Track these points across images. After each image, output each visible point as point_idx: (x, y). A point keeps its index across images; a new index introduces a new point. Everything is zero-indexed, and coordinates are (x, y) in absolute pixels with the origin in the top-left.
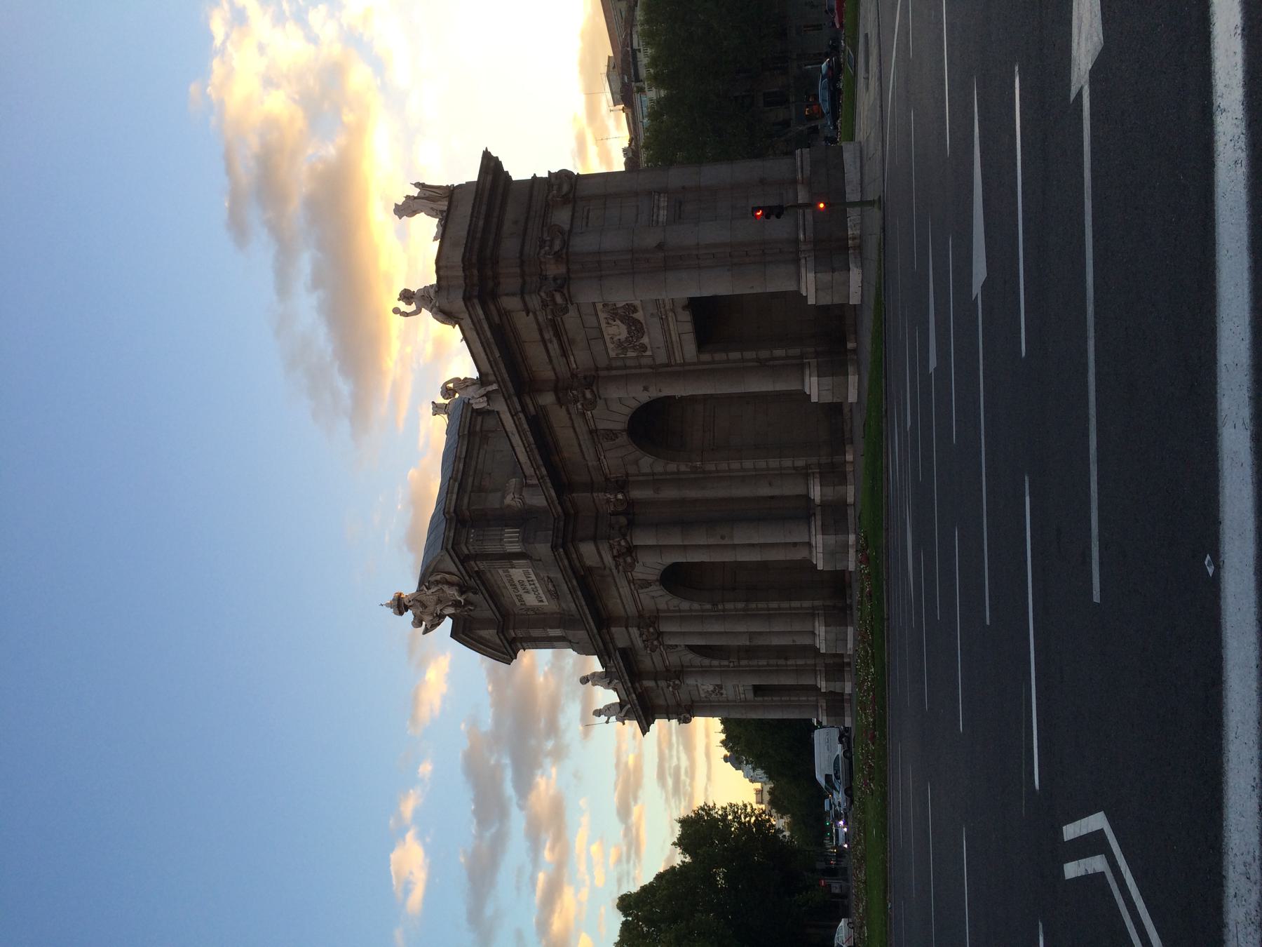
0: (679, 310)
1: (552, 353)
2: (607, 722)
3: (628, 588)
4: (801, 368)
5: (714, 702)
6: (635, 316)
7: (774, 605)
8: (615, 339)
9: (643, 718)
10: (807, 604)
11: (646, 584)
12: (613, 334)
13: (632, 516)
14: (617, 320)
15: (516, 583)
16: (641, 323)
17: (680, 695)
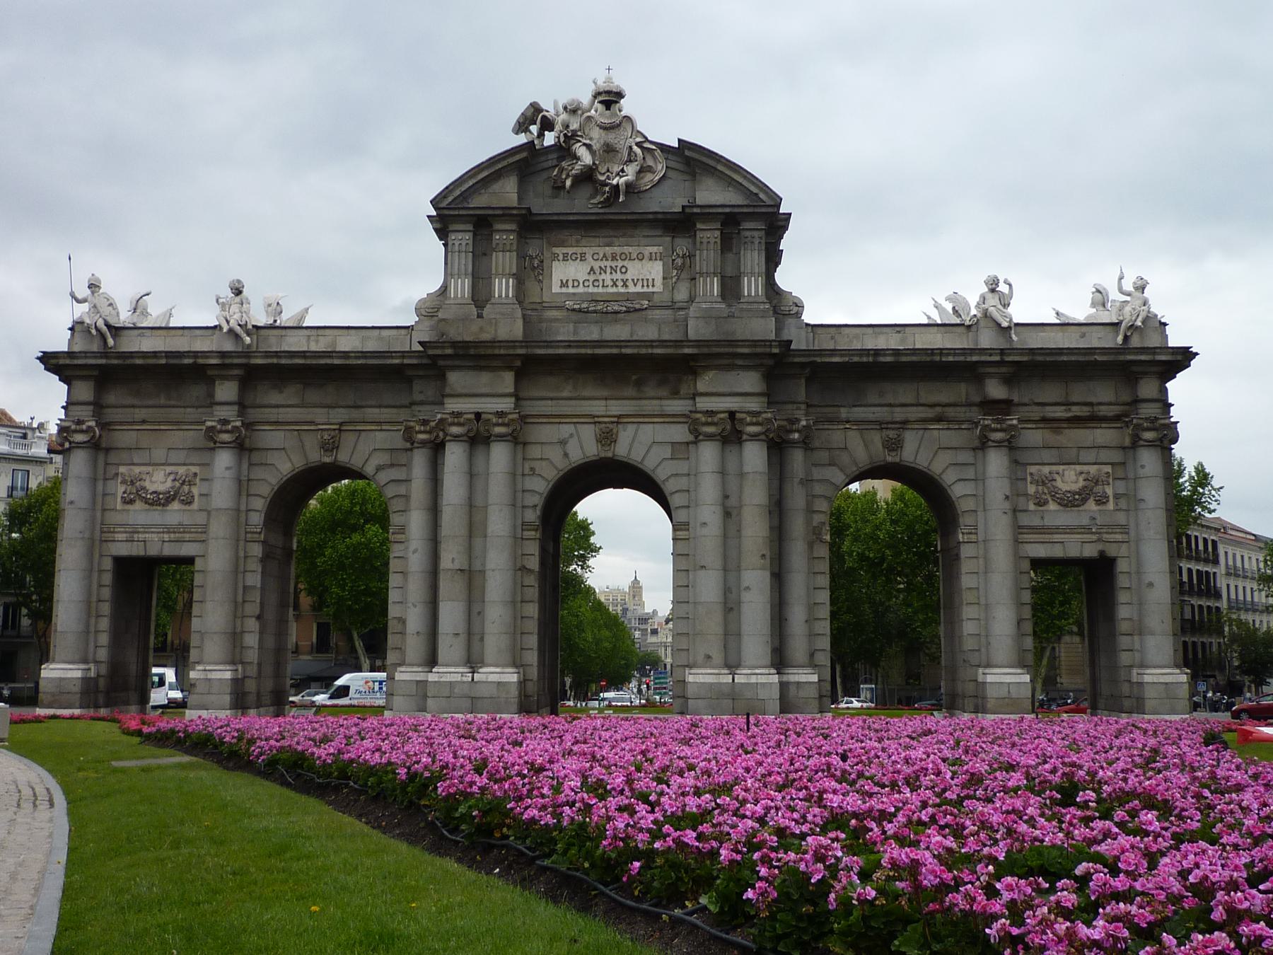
0: (1100, 547)
1: (1048, 408)
2: (73, 296)
3: (603, 413)
4: (1021, 664)
5: (104, 485)
6: (1092, 498)
7: (533, 610)
8: (1056, 476)
9: (115, 362)
10: (532, 658)
11: (607, 438)
12: (1063, 475)
13: (777, 447)
14: (1084, 483)
15: (620, 263)
16: (1080, 506)
17: (134, 434)
